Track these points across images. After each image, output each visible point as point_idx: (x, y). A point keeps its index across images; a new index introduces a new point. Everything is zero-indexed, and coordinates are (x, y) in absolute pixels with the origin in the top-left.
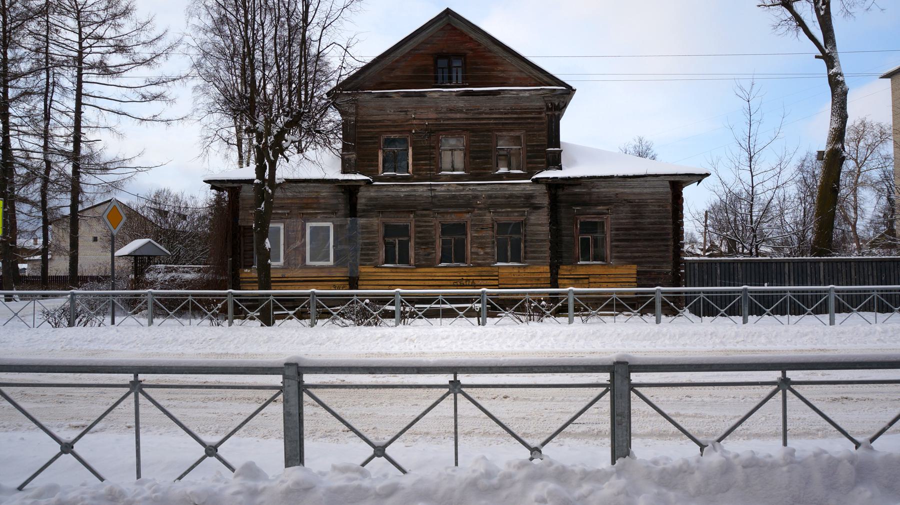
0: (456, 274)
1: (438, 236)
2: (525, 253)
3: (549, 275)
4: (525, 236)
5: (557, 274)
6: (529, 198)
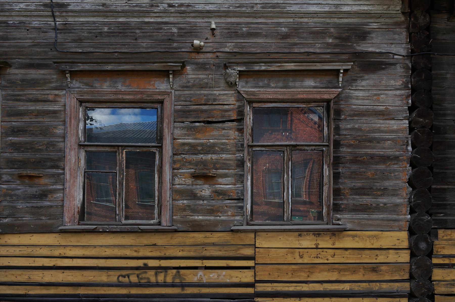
0: (128, 253)
1: (71, 141)
2: (337, 193)
3: (405, 257)
4: (337, 144)
5: (430, 254)
6: (347, 39)
